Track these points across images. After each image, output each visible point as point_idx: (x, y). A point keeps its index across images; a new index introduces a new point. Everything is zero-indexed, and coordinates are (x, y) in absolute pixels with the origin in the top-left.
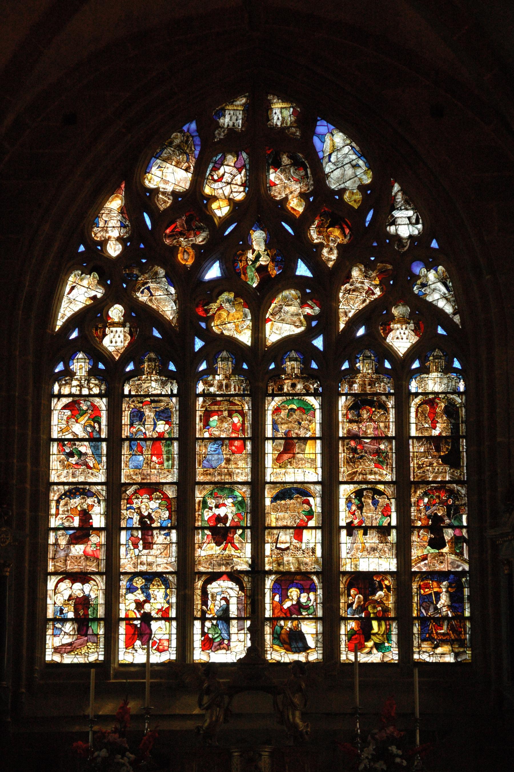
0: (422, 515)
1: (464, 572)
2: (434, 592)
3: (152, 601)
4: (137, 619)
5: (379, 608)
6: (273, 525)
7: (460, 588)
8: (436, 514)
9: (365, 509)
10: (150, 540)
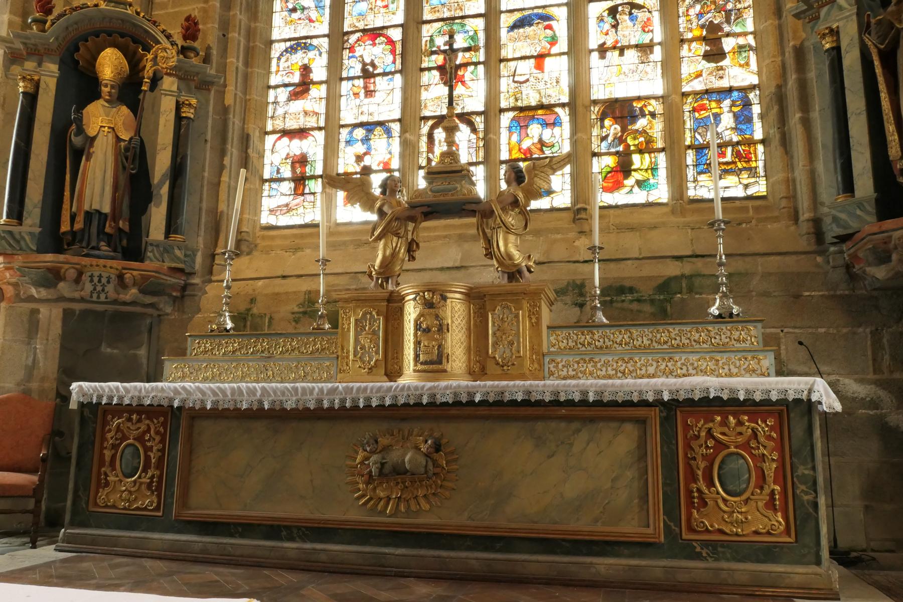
0: (694, 25)
1: (753, 87)
2: (713, 114)
3: (373, 152)
4: (356, 173)
5: (642, 139)
6: (510, 57)
7: (747, 104)
8: (711, 21)
9: (620, 27)
10: (372, 88)
